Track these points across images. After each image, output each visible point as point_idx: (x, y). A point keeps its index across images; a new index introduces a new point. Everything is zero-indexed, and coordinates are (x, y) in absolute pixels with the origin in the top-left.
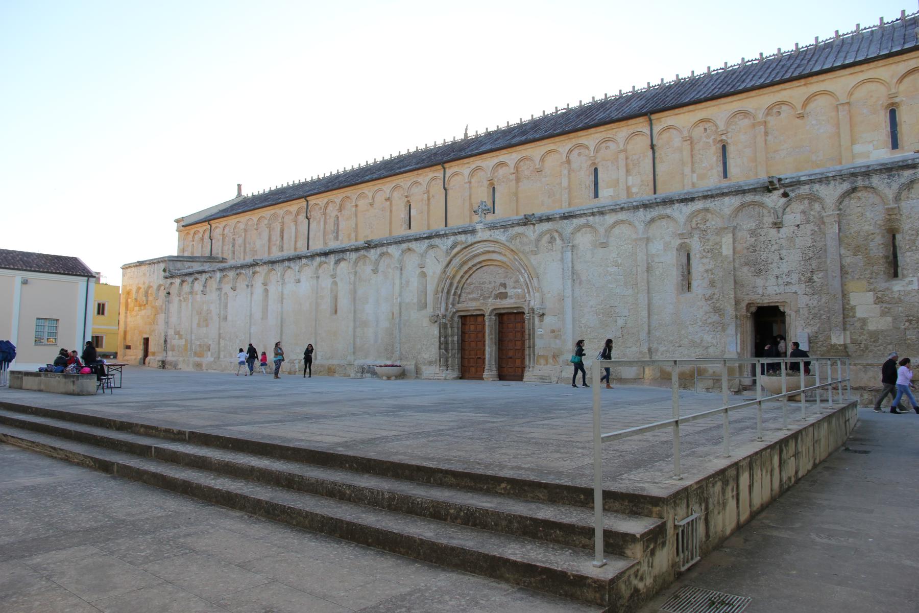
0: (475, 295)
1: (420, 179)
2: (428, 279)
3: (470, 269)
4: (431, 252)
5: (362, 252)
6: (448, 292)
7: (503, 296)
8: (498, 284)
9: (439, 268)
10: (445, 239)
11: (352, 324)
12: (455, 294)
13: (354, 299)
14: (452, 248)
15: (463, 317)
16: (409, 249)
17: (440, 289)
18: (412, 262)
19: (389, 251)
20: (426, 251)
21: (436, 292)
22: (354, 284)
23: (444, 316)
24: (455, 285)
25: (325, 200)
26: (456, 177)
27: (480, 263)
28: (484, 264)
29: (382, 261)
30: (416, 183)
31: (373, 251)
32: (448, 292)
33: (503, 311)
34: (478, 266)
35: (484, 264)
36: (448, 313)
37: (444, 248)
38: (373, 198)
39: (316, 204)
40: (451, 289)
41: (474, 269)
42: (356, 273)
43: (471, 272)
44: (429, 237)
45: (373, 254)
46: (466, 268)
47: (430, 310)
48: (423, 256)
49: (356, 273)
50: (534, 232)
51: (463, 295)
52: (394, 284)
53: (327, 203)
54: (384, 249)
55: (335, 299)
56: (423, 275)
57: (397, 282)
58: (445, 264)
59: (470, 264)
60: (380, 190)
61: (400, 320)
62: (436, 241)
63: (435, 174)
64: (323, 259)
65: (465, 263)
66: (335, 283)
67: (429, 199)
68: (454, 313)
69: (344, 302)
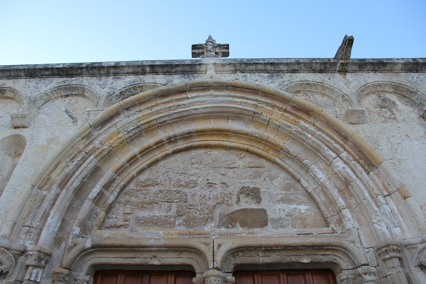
0: (157, 213)
3: (160, 144)
4: (61, 104)
6: (80, 192)
8: (235, 188)
9: (69, 132)
10: (110, 79)
12: (99, 199)
17: (57, 177)
21: (44, 182)
23: (44, 258)
24: (108, 173)
27: (188, 136)
28: (197, 141)
32: (80, 192)
33: (262, 259)
34: (181, 145)
35: (197, 141)
36: (57, 253)
37: (104, 92)
41: (169, 149)
43: (158, 154)
46: (149, 141)
50: (348, 83)
59: (162, 135)
68: (85, 253)
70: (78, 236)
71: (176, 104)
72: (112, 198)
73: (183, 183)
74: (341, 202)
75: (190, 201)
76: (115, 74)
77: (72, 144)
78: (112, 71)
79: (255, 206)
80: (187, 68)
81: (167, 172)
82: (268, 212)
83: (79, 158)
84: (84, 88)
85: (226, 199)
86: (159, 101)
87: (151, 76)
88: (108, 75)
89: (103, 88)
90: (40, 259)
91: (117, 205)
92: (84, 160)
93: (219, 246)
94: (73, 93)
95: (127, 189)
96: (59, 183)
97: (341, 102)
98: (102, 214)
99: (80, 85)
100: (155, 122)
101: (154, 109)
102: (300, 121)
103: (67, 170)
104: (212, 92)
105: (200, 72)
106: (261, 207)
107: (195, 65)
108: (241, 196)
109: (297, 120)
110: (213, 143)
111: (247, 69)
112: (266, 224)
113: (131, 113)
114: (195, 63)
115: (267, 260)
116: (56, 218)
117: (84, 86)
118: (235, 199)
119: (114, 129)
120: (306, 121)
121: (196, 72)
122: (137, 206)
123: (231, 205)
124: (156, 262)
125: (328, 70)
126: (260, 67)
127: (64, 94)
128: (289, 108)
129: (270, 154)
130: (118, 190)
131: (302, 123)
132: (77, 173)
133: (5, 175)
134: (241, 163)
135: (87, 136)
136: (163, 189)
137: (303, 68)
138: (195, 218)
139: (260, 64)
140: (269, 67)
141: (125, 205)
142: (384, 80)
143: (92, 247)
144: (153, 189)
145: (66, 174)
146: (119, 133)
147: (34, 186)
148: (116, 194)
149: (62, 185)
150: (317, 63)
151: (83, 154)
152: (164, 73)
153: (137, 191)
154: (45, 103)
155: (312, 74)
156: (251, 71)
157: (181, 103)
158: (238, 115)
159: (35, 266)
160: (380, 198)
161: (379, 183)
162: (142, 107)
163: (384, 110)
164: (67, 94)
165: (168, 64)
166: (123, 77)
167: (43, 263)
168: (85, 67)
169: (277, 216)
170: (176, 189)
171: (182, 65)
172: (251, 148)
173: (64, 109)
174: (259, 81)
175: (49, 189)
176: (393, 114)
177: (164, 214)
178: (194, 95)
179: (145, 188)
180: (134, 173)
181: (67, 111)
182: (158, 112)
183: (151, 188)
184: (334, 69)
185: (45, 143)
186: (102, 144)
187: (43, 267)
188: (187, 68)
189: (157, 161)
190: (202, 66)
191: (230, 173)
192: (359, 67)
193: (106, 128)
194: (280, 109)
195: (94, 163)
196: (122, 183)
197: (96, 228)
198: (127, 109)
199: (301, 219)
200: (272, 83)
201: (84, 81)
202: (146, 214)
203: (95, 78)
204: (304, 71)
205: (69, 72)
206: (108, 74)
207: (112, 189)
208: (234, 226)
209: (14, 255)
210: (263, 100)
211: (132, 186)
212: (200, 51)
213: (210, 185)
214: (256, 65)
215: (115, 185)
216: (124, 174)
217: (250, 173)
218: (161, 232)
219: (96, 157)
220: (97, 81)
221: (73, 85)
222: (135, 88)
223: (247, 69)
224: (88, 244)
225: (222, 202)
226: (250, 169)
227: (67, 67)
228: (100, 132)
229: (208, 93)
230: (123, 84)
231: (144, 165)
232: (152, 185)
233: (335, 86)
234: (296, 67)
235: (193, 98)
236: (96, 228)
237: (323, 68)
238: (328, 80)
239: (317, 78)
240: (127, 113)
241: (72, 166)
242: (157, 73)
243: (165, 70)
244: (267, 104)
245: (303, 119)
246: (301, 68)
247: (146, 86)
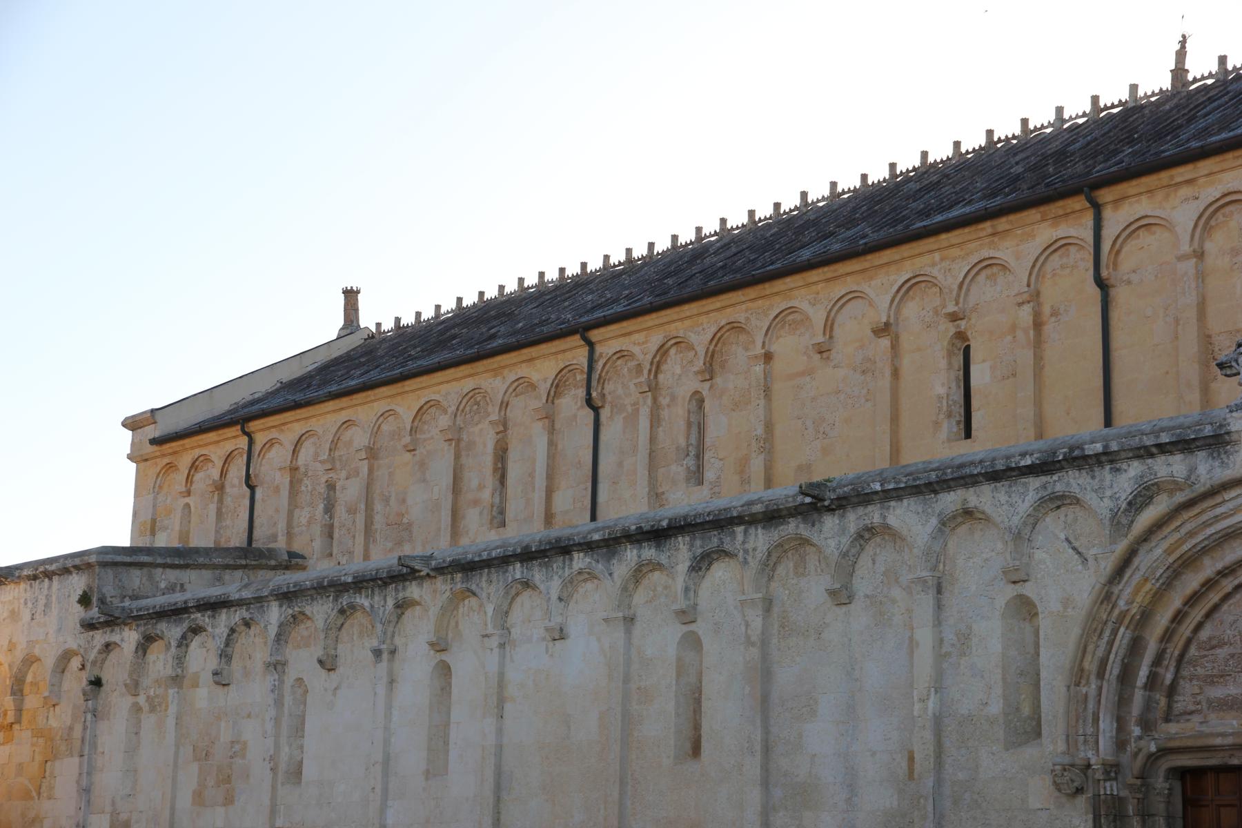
1: (1005, 251)
2: (1044, 623)
3: (1209, 584)
4: (1054, 525)
5: (792, 527)
9: (1083, 585)
10: (1106, 473)
11: (754, 796)
13: (765, 700)
15: (1183, 774)
16: (967, 513)
17: (1090, 665)
18: (977, 561)
19: (892, 520)
20: (1033, 521)
21: (1078, 676)
22: (764, 642)
23: (1112, 770)
25: (656, 340)
26: (1144, 238)
29: (865, 560)
30: (987, 265)
31: (830, 522)
36: (1125, 759)
37: (1103, 507)
38: (829, 326)
39: (621, 354)
40: (1137, 658)
42: (768, 605)
43: (1214, 597)
44: (1046, 467)
45: (832, 533)
46: (1192, 581)
47: (1053, 745)
48: (1020, 537)
49: (768, 605)
51: (1187, 689)
52: (912, 644)
53: (662, 351)
54: (873, 515)
55: (694, 701)
56: (1025, 609)
57: (925, 636)
58: (1108, 565)
59: (1209, 567)
60: (854, 296)
61: (939, 782)
62: (1073, 481)
63: (1063, 230)
64: (649, 552)
65: (1188, 562)
66: (693, 642)
67: (1038, 325)
68: (1153, 758)
69: (726, 716)
70: (1140, 738)
71: (1210, 514)
72: (1169, 677)
76: (1111, 462)
77: (1091, 617)
78: (1104, 458)
80: (1211, 441)
81: (1235, 622)
83: (1107, 633)
86: (1185, 515)
87: (1163, 458)
88: (1100, 464)
90: (1107, 773)
91: (1182, 682)
92: (1115, 632)
95: (1187, 657)
98: (1163, 702)
100: (1190, 553)
101: (1183, 531)
103: (1100, 653)
107: (1221, 435)
113: (1153, 544)
116: (1108, 720)
119: (1137, 577)
121: (1228, 443)
122: (1205, 681)
130: (1173, 663)
132: (1112, 656)
133: (1032, 651)
135: (1106, 597)
136: (1234, 651)
141: (1191, 680)
143: (1158, 751)
144: (1222, 653)
146: (1146, 580)
147: (1069, 687)
148: (1172, 669)
149: (1101, 675)
151: (1110, 626)
157: (1219, 511)
159: (1105, 780)
162: (1166, 530)
166: (1124, 466)
167: (1113, 775)
173: (1062, 536)
175: (1088, 683)
180: (1188, 633)
181: (1067, 540)
182: (1191, 534)
183: (1218, 651)
186: (1130, 602)
187: (1116, 779)
188: (1211, 441)
189: (1216, 608)
193: (1126, 578)
195: (1128, 635)
196: (1177, 653)
197: (1159, 722)
198: (1145, 540)
202: (1217, 692)
203: (1084, 472)
207: (1166, 663)
209: (1081, 770)
211: (1193, 651)
215: (1167, 656)
216: (1176, 639)
218: (1235, 722)
219: (1127, 628)
220: (1089, 480)
222: (1147, 488)
224: (1153, 748)
228: (1120, 587)
231: (1199, 618)
232: (1220, 647)
236: (1159, 722)
240: (1146, 546)
241: (1103, 643)
242: (1171, 453)
243: (1180, 447)
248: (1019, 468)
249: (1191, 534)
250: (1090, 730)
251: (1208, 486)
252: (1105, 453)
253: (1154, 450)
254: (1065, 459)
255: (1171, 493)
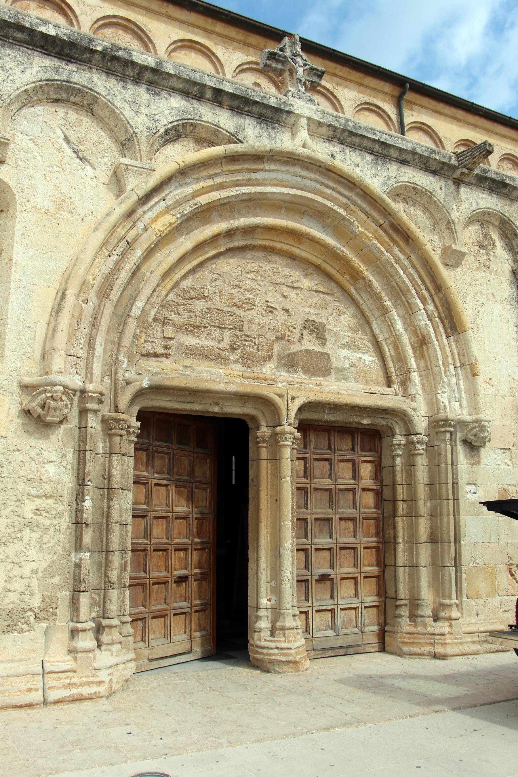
7: (318, 365)
8: (297, 320)
14: (175, 134)
27: (249, 231)
33: (328, 417)
34: (238, 243)
73: (236, 301)
74: (413, 363)
75: (246, 331)
78: (148, 75)
79: (317, 348)
80: (268, 113)
82: (333, 359)
83: (119, 251)
84: (97, 98)
85: (288, 333)
88: (137, 80)
89: (136, 113)
93: (293, 398)
94: (72, 99)
96: (97, 289)
97: (443, 228)
99: (90, 89)
101: (218, 180)
102: (395, 247)
104: (298, 170)
105: (285, 123)
106: (324, 351)
108: (305, 332)
109: (391, 244)
110: (278, 245)
111: (349, 140)
112: (329, 373)
114: (282, 107)
115: (331, 418)
117: (98, 93)
118: (297, 335)
120: (401, 250)
121: (278, 122)
123: (293, 343)
124: (216, 409)
125: (443, 172)
126: (366, 143)
127: (55, 97)
128: (386, 225)
129: (345, 280)
131: (396, 250)
134: (306, 283)
136: (213, 306)
137: (417, 160)
138: (252, 354)
139: (369, 138)
140: (377, 147)
142: (496, 208)
144: (200, 305)
145: (104, 276)
150: (436, 159)
152: (232, 109)
153: (178, 304)
154: (20, 109)
155: (423, 172)
156: (353, 146)
157: (253, 176)
158: (320, 215)
160: (451, 367)
161: (455, 351)
163: (482, 251)
164: (58, 97)
165: (243, 95)
166: (164, 94)
168: (100, 52)
169: (340, 365)
170: (228, 309)
171: (263, 104)
172: (324, 265)
174: (360, 169)
176: (489, 260)
177: (214, 344)
178: (273, 167)
179: (190, 302)
181: (67, 140)
183: (196, 302)
184: (449, 174)
185: (49, 205)
188: (268, 113)
190: (292, 115)
191: (293, 295)
192: (478, 180)
193: (153, 202)
194: (375, 221)
199: (365, 372)
200: (376, 175)
201: (96, 80)
202: (190, 341)
204: (415, 166)
205: (67, 51)
206: (138, 79)
208: (295, 372)
210: (359, 202)
212: (280, 66)
213: (271, 310)
214: (362, 139)
217: (315, 300)
221: (76, 84)
223: (349, 140)
224: (146, 383)
225: (283, 338)
226: (316, 294)
227: (65, 38)
229: (292, 169)
230: (167, 112)
233: (444, 204)
234: (409, 157)
235: (270, 171)
237: (439, 168)
238: (438, 189)
239: (428, 182)
242: (220, 105)
243: (236, 103)
244: (363, 210)
245: (398, 246)
246: (414, 160)
247: (203, 126)
248: (32, 32)
249: (221, 187)
250: (82, 353)
251: (268, 148)
252: (154, 71)
253: (209, 94)
254: (103, 54)
255: (201, 142)
